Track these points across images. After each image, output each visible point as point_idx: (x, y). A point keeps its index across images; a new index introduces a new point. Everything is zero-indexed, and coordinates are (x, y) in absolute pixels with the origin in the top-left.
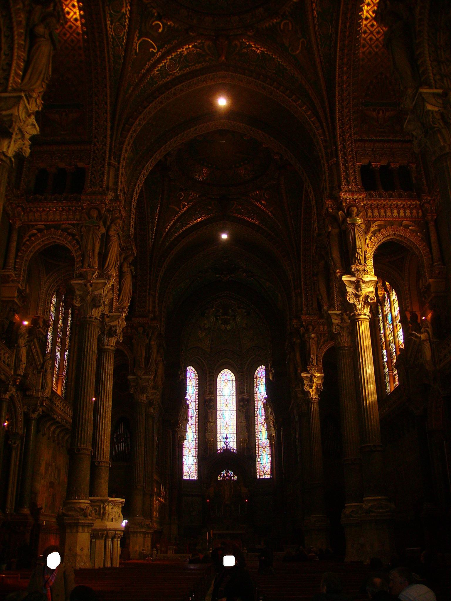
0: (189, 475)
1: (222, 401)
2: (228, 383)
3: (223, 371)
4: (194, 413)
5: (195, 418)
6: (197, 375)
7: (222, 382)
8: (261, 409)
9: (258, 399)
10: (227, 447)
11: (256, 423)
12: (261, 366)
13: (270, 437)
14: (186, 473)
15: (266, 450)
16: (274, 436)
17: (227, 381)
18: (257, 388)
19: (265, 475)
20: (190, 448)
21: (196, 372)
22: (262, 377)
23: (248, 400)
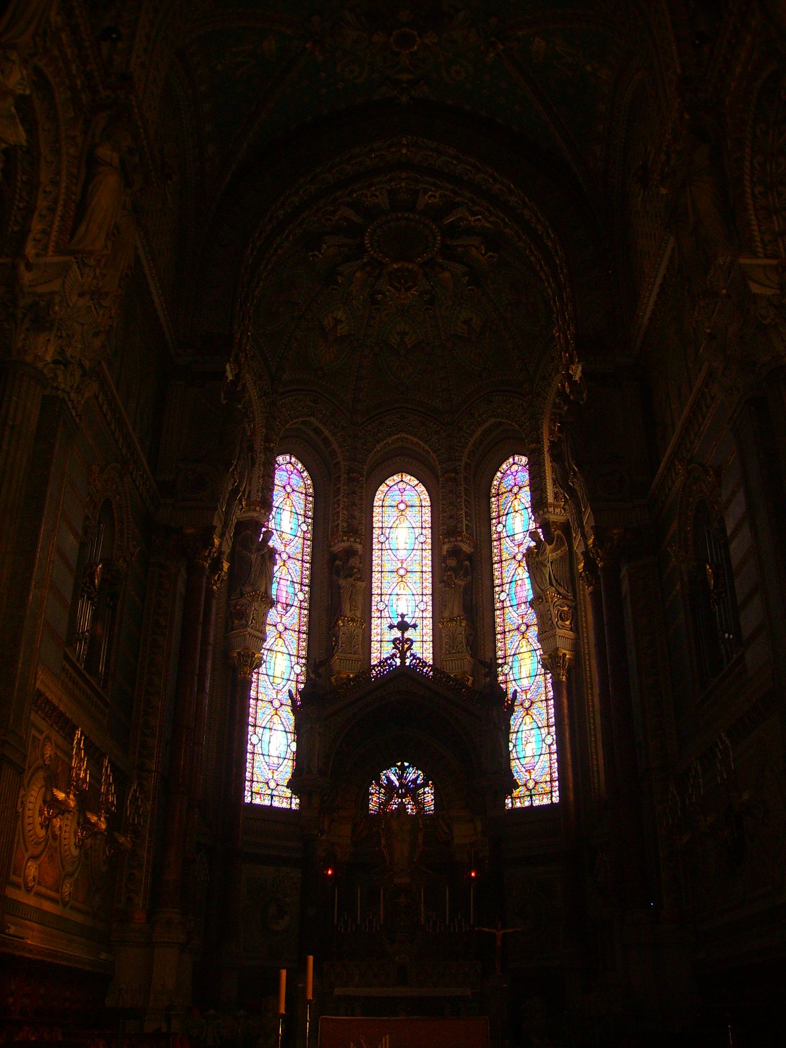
0: (269, 792)
1: (387, 567)
2: (408, 512)
3: (391, 478)
4: (296, 595)
5: (297, 611)
6: (309, 482)
7: (388, 511)
8: (513, 584)
9: (505, 556)
10: (403, 658)
11: (499, 629)
12: (511, 460)
13: (550, 662)
14: (261, 785)
15: (533, 711)
16: (565, 655)
17: (402, 508)
18: (499, 523)
19: (531, 796)
20: (277, 704)
21: (305, 474)
22: (515, 489)
23: (470, 557)
